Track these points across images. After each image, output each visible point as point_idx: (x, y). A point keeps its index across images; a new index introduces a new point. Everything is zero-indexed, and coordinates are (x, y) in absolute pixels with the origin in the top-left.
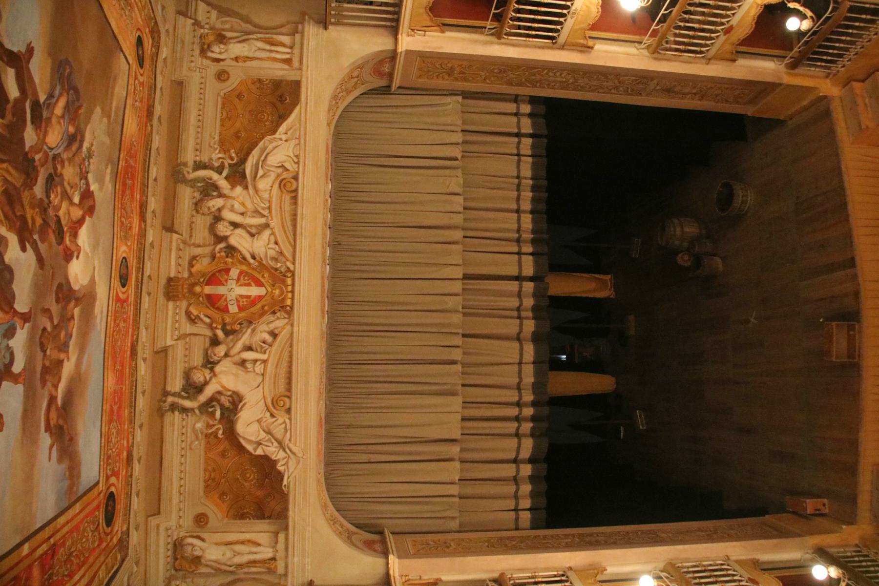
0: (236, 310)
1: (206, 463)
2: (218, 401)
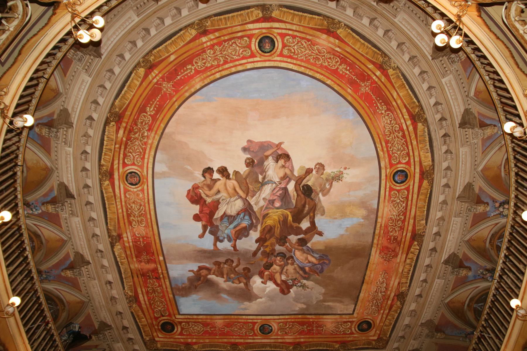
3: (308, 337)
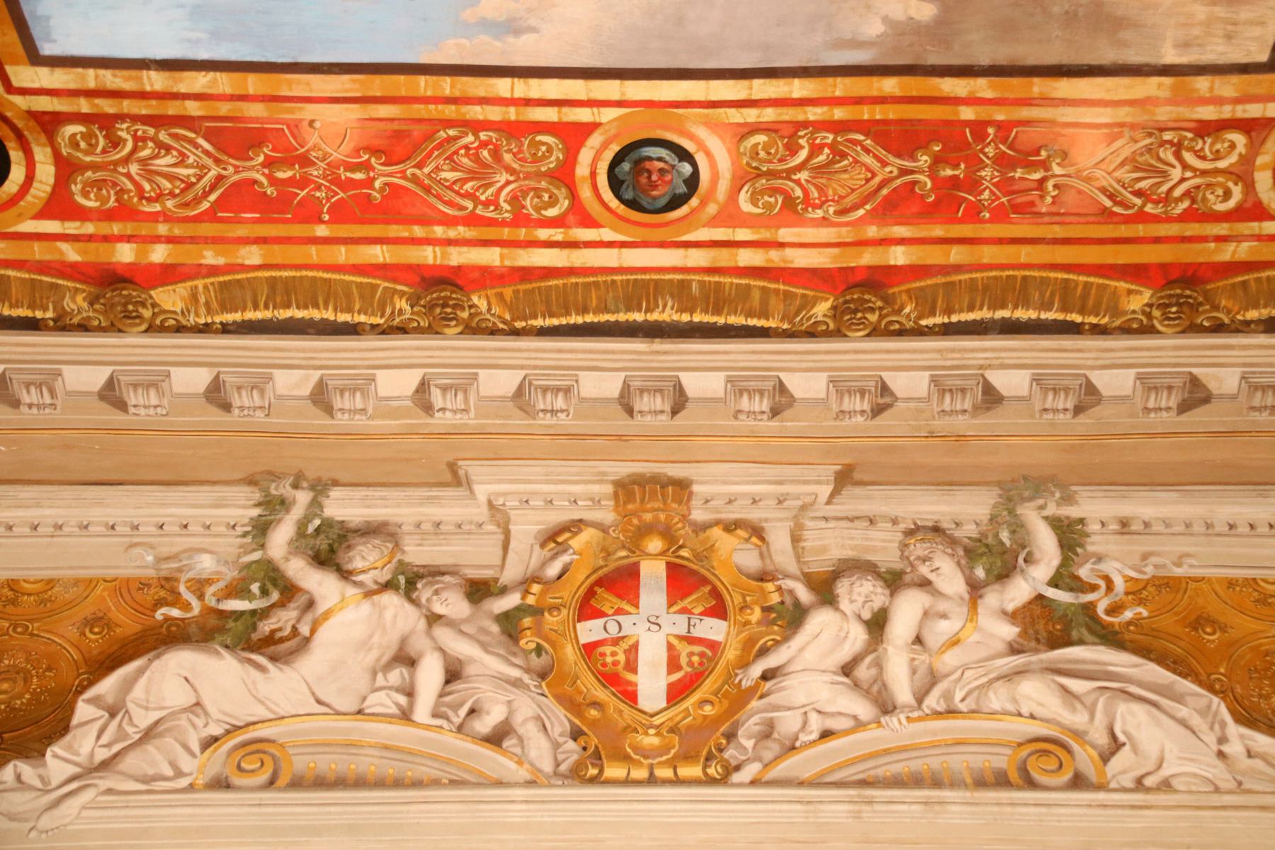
0: (583, 640)
1: (77, 582)
2: (281, 604)
3: (938, 231)
